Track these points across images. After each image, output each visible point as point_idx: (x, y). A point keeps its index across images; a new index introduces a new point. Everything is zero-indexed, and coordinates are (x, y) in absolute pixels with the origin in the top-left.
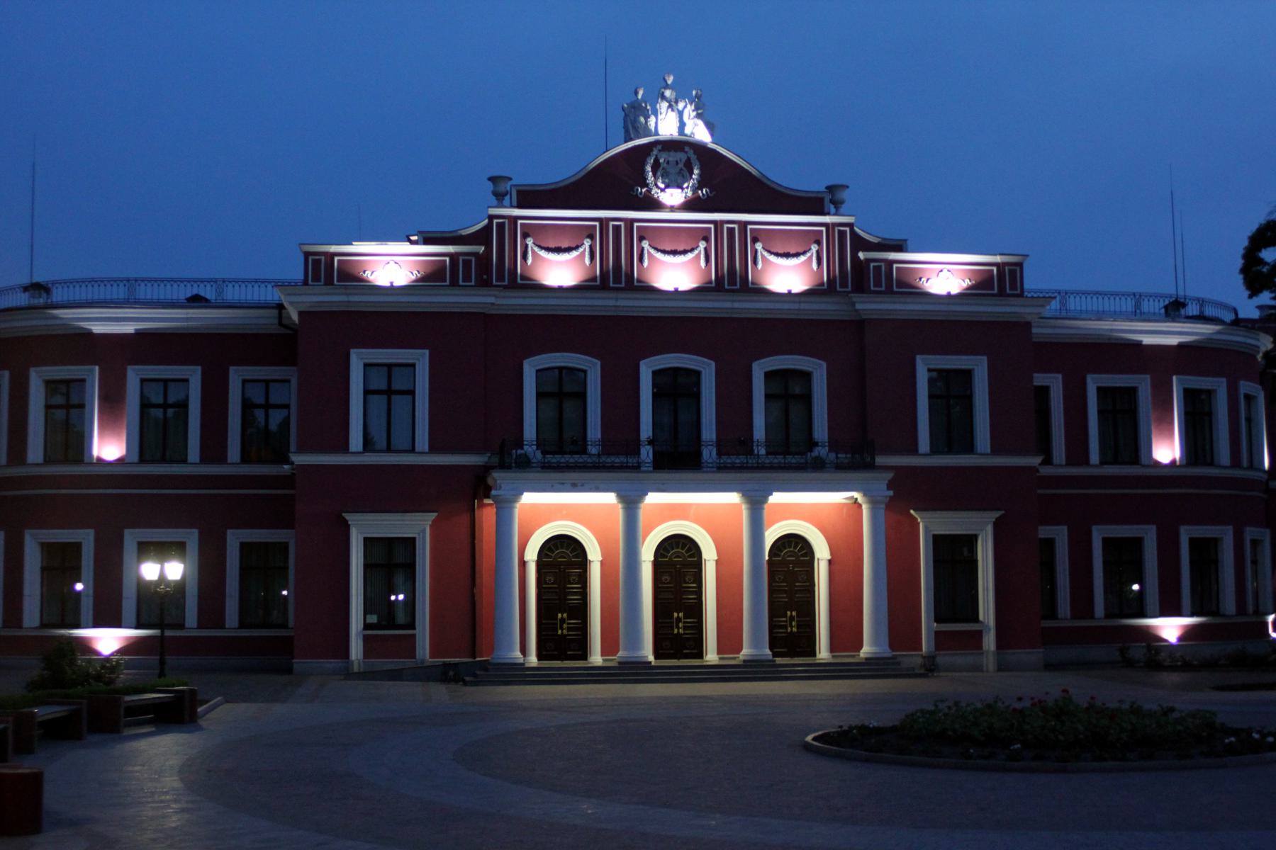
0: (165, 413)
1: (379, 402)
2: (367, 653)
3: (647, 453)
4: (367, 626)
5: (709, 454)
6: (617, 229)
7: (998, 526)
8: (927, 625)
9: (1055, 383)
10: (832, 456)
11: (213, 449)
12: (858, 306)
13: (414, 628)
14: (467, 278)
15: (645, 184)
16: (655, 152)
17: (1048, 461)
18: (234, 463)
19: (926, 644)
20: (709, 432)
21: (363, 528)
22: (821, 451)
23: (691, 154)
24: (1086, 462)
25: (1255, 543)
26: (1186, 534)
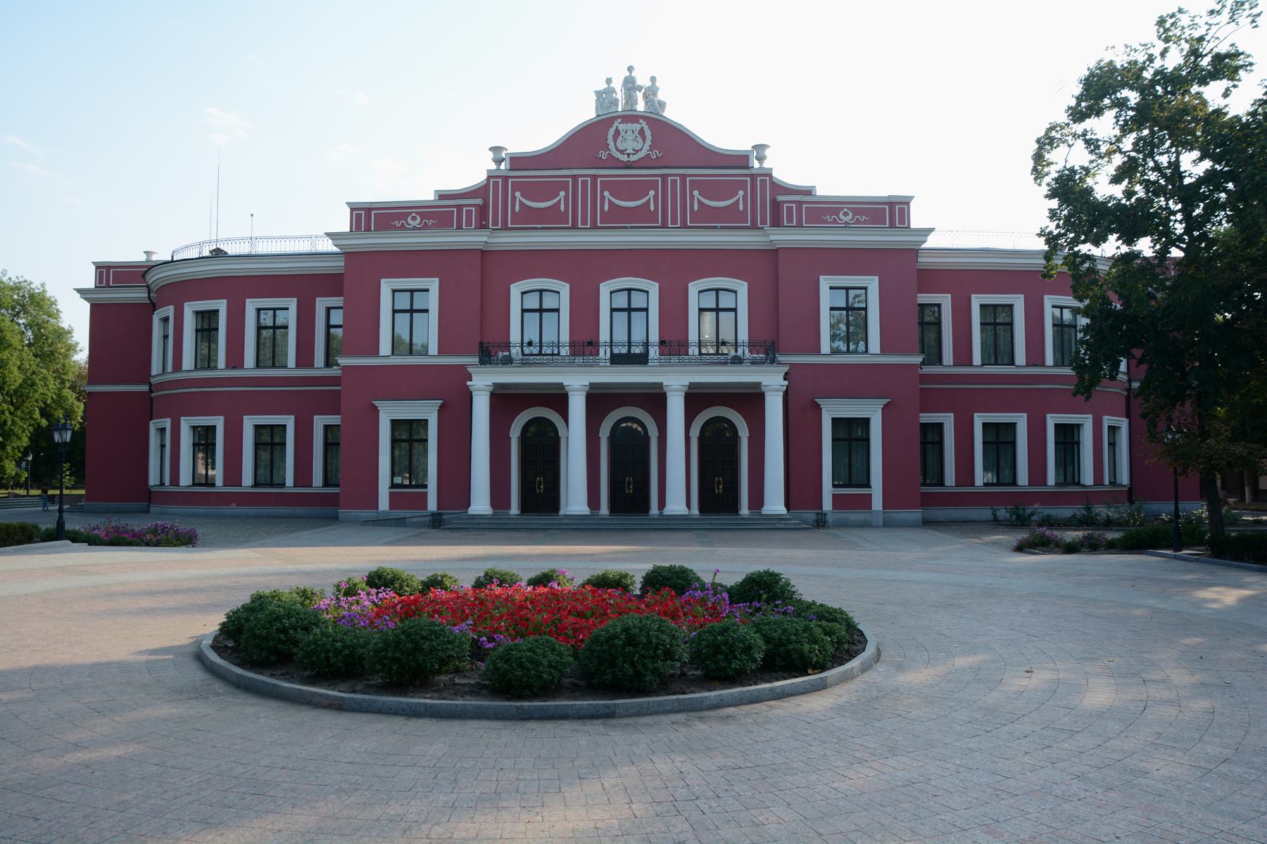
0: (274, 333)
1: (403, 319)
2: (392, 506)
4: (393, 486)
5: (654, 352)
6: (584, 183)
11: (305, 358)
12: (772, 238)
14: (469, 223)
15: (607, 148)
16: (616, 124)
18: (319, 367)
19: (827, 505)
21: (388, 412)
22: (743, 351)
23: (644, 124)
24: (970, 364)
25: (1113, 430)
26: (1052, 420)
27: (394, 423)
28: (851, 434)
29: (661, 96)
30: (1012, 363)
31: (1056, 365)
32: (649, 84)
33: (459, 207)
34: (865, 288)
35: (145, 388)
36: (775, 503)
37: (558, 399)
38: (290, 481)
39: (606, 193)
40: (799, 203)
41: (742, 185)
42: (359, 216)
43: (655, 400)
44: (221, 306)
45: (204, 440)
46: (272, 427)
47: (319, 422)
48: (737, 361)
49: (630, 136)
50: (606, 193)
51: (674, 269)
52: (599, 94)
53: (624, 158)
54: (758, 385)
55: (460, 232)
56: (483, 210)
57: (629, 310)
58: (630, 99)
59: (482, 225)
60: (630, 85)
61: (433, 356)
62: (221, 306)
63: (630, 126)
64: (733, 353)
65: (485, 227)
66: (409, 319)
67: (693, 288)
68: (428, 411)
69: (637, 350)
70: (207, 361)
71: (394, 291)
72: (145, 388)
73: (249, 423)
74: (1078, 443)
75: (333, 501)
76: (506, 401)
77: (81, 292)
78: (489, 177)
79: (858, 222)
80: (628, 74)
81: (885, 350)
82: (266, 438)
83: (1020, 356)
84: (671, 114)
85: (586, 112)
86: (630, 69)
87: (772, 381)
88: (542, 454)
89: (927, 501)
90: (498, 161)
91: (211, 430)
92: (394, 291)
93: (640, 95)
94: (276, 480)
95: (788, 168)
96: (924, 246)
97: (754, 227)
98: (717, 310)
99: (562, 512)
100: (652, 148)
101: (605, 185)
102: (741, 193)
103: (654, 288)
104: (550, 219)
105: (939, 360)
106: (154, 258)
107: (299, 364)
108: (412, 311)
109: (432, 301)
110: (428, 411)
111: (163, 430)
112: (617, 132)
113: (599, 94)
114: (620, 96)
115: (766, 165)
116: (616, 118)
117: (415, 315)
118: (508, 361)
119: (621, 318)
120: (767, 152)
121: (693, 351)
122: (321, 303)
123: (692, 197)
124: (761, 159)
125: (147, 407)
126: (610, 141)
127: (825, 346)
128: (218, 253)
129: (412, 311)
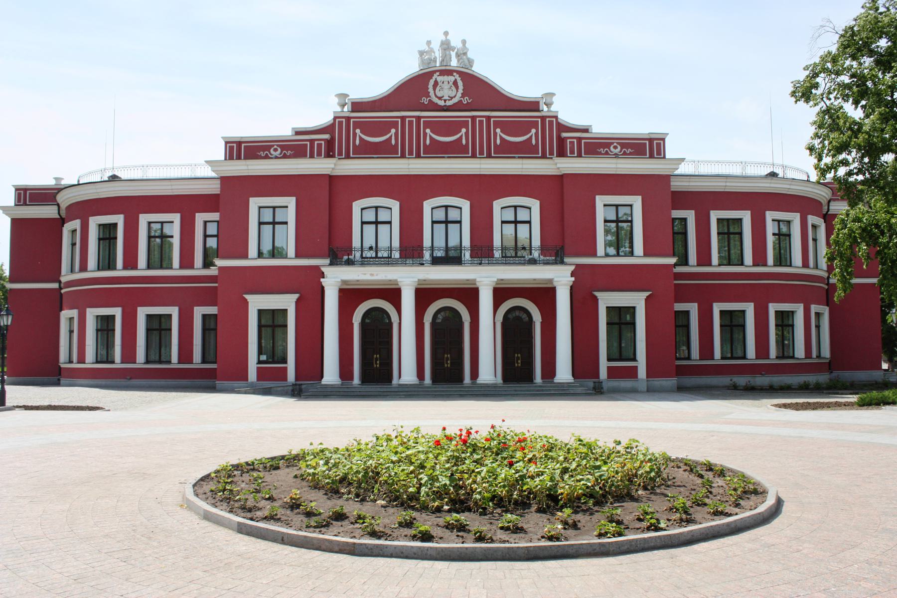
1: (267, 229)
3: (427, 255)
4: (259, 362)
5: (467, 255)
7: (647, 299)
8: (604, 364)
9: (690, 216)
10: (542, 257)
11: (187, 261)
12: (559, 165)
13: (286, 362)
15: (428, 95)
16: (435, 76)
17: (684, 261)
18: (198, 271)
20: (466, 242)
21: (257, 302)
22: (536, 254)
23: (457, 76)
25: (818, 315)
26: (773, 308)
27: (261, 312)
28: (622, 319)
29: (469, 55)
30: (742, 264)
31: (775, 265)
32: (460, 45)
33: (312, 141)
34: (631, 206)
35: (55, 286)
36: (564, 372)
37: (393, 295)
38: (175, 358)
39: (428, 131)
40: (579, 139)
41: (534, 125)
42: (231, 148)
43: (469, 295)
44: (119, 220)
45: (105, 325)
46: (160, 316)
47: (199, 312)
48: (533, 262)
49: (446, 86)
50: (428, 131)
51: (482, 191)
52: (421, 53)
53: (441, 103)
54: (551, 281)
55: (312, 160)
56: (330, 144)
57: (447, 222)
58: (446, 58)
59: (330, 154)
60: (446, 46)
61: (292, 261)
62: (119, 220)
63: (446, 78)
64: (528, 257)
65: (333, 156)
66: (274, 231)
67: (497, 205)
68: (287, 302)
69: (452, 254)
70: (107, 262)
71: (260, 208)
72: (55, 286)
73: (142, 313)
74: (793, 326)
75: (210, 375)
76: (350, 296)
77: (5, 209)
78: (335, 118)
79: (625, 154)
80: (444, 38)
81: (646, 254)
82: (155, 325)
83: (748, 258)
84: (480, 69)
85: (411, 67)
86: (446, 33)
87: (561, 277)
88: (378, 334)
89: (681, 371)
90: (343, 106)
91: (113, 317)
92: (260, 208)
93: (453, 54)
94: (163, 359)
95: (569, 111)
96: (677, 172)
97: (544, 157)
98: (516, 222)
99: (395, 381)
100: (463, 95)
101: (427, 124)
102: (534, 131)
103: (466, 205)
104: (384, 150)
105: (686, 263)
106: (63, 182)
107: (182, 267)
108: (274, 223)
109: (291, 216)
110: (287, 302)
111: (71, 319)
112: (436, 84)
113: (421, 53)
114: (438, 54)
115: (553, 108)
116: (435, 72)
117: (276, 226)
118: (350, 263)
119: (440, 229)
120: (554, 99)
121: (497, 254)
122: (200, 218)
123: (495, 134)
124: (548, 105)
125: (57, 301)
126: (431, 90)
127: (600, 250)
128: (114, 178)
129: (274, 223)
